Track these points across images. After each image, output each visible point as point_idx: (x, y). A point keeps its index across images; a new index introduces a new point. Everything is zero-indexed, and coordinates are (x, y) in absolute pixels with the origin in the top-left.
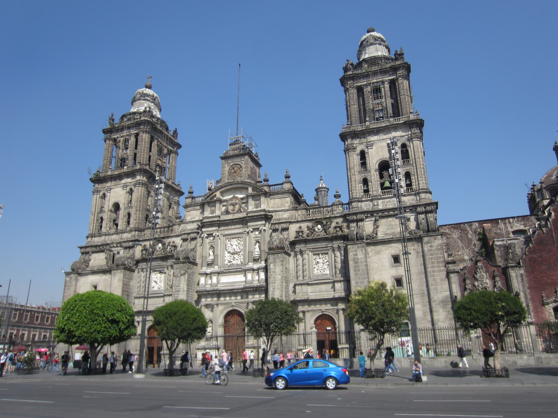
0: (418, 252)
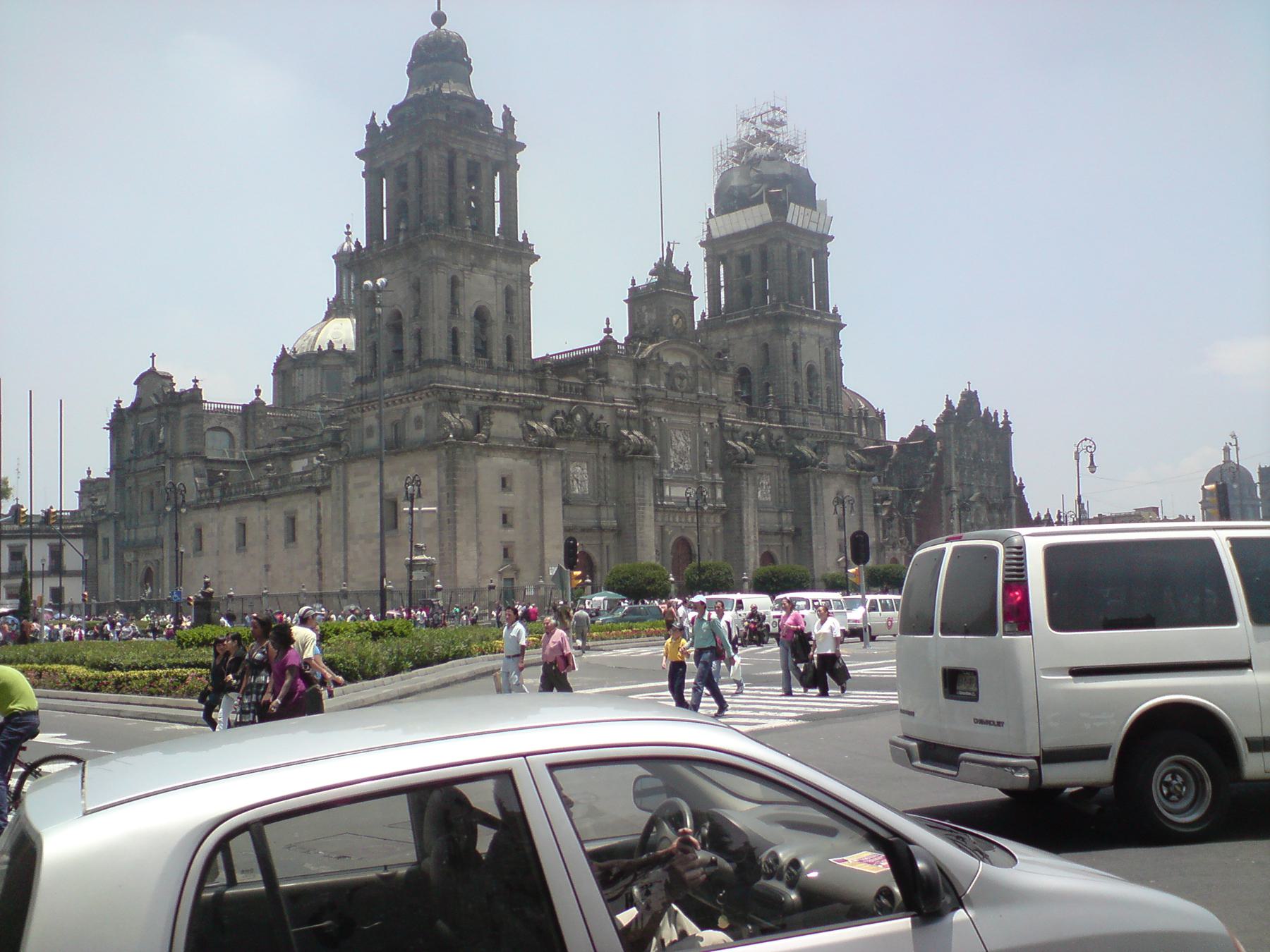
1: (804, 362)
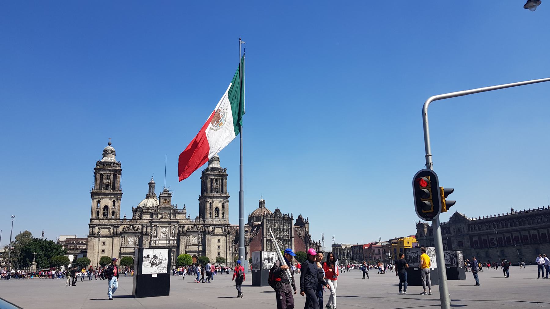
0: (225, 239)
1: (214, 207)
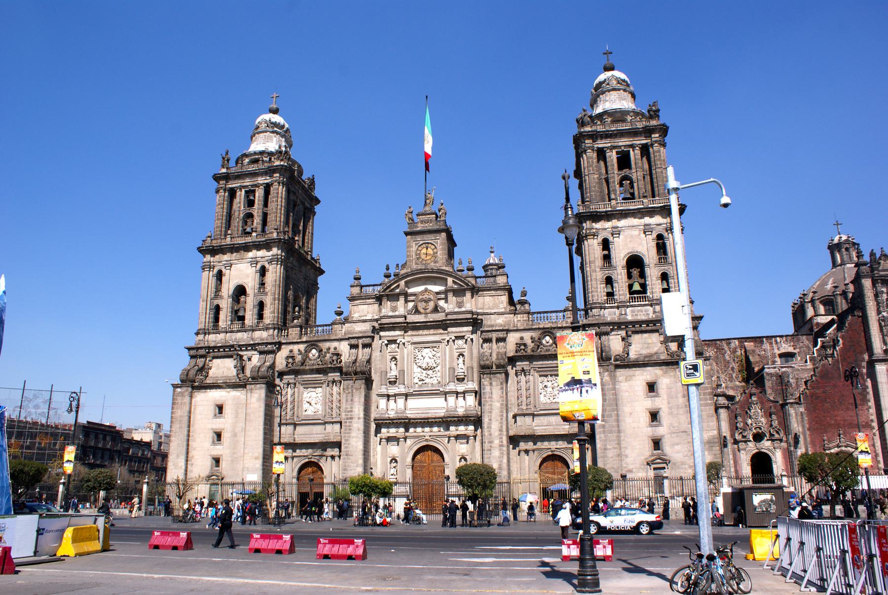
1: (620, 253)
